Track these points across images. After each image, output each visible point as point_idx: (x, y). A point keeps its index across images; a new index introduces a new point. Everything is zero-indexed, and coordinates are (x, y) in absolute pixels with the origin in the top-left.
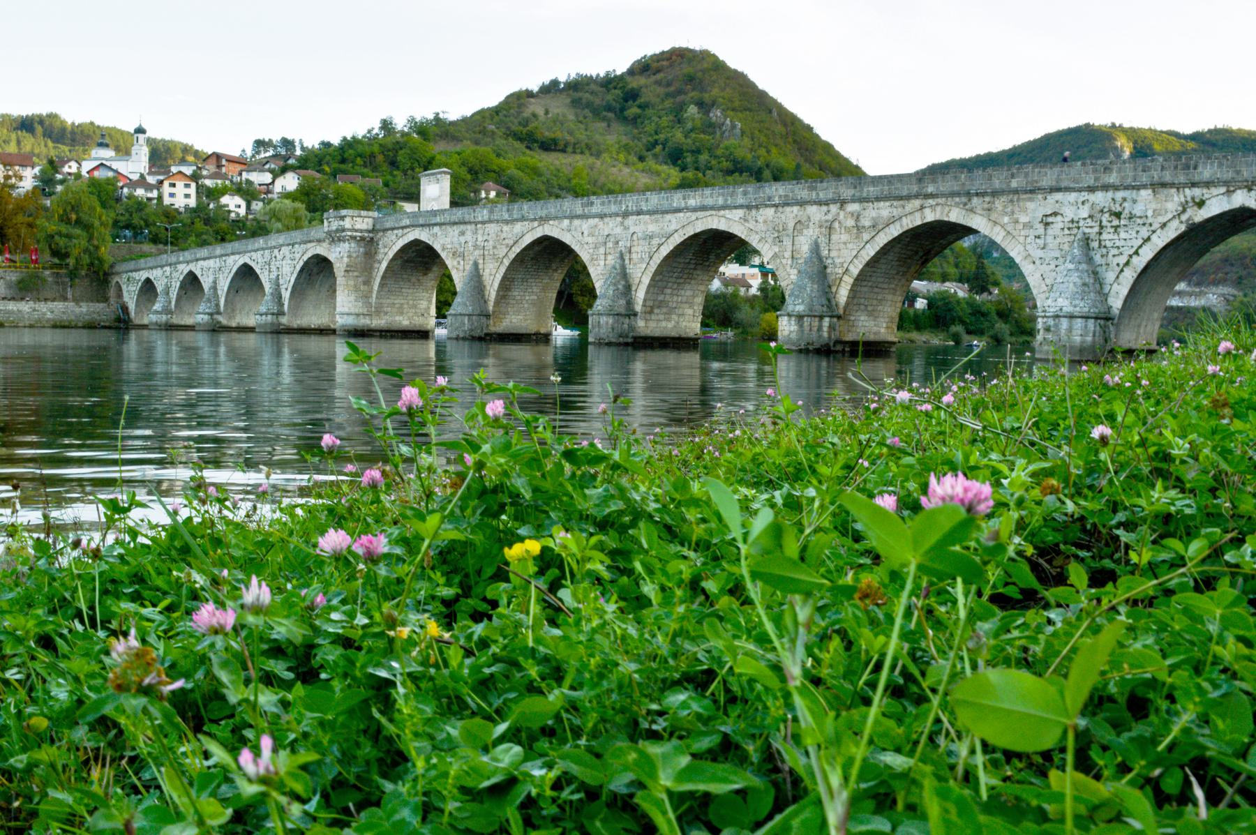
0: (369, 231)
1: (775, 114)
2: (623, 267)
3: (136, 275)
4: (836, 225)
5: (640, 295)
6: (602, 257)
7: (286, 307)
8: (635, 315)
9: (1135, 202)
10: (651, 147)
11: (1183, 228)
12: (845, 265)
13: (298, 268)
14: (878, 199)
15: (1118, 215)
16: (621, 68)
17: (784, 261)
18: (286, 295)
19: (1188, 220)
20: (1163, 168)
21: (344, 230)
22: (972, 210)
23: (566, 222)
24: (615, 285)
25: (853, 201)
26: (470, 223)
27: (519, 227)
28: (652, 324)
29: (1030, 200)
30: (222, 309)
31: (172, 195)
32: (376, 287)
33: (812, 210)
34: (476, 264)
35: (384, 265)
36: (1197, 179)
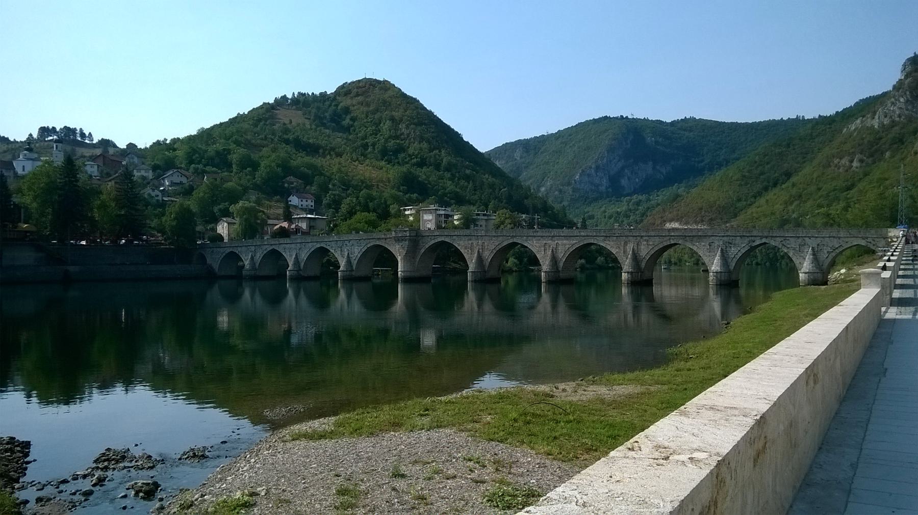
0: (415, 236)
3: (222, 250)
5: (561, 265)
7: (354, 267)
8: (559, 271)
9: (736, 240)
10: (365, 146)
11: (749, 248)
15: (730, 243)
16: (331, 90)
18: (355, 263)
20: (743, 231)
21: (407, 236)
22: (686, 241)
33: (631, 238)
34: (478, 252)
35: (423, 251)
36: (752, 235)
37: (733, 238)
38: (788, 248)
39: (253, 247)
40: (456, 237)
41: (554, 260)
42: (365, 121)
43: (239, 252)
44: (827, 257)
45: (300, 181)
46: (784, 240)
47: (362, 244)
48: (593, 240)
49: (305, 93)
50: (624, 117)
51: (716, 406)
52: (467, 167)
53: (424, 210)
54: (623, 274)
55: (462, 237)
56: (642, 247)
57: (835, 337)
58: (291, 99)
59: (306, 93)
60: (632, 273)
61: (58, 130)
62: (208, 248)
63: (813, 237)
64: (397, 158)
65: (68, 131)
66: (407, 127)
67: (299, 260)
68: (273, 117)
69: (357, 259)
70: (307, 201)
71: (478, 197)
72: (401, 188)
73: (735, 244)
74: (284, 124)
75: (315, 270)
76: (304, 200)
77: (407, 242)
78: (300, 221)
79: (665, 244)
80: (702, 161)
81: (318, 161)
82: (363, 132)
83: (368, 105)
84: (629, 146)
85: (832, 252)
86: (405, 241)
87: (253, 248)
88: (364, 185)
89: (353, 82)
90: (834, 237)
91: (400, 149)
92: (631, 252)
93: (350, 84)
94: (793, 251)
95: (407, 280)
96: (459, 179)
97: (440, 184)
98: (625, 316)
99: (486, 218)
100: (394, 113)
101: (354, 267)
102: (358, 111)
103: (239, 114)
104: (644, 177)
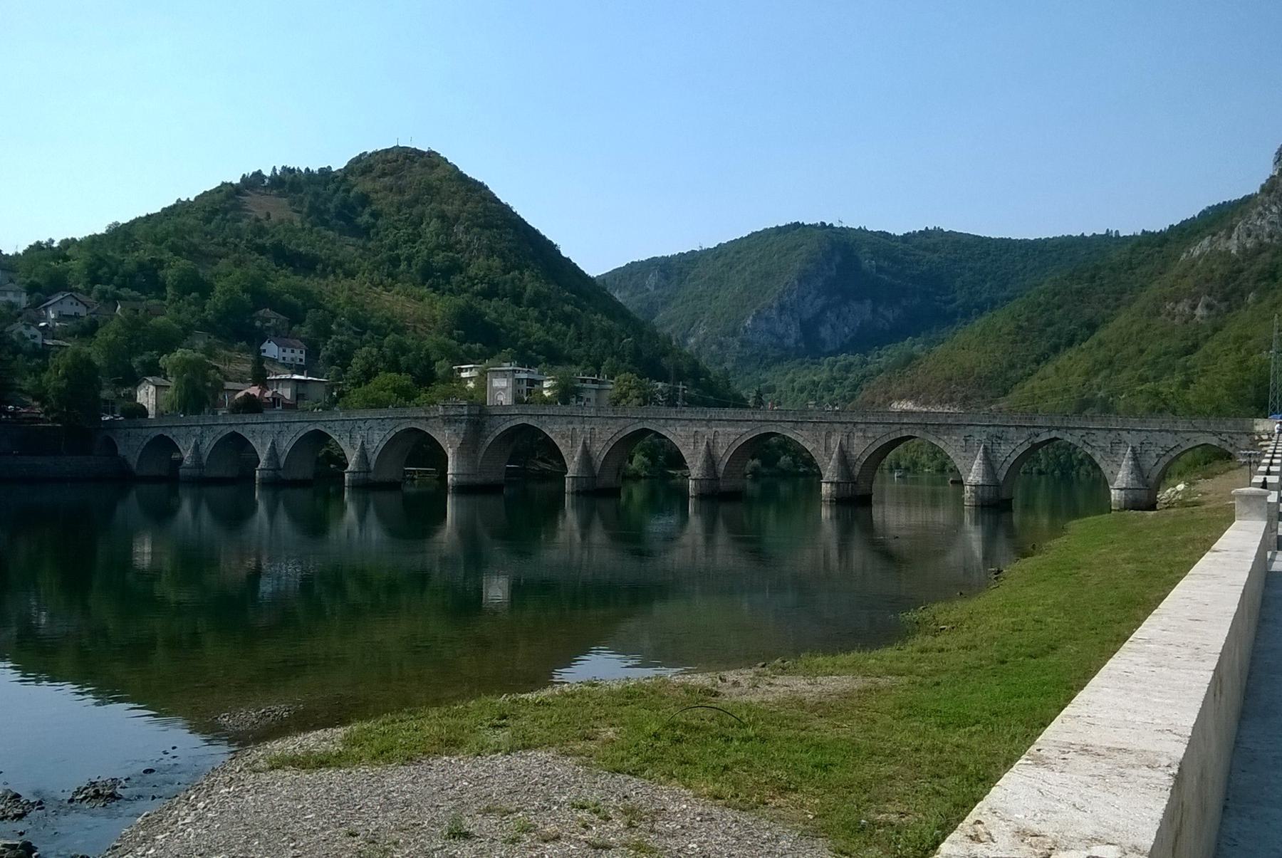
3: (144, 432)
4: (852, 434)
5: (722, 468)
7: (372, 466)
10: (395, 261)
13: (389, 437)
14: (876, 423)
16: (338, 164)
18: (373, 458)
21: (463, 415)
25: (861, 423)
27: (622, 421)
29: (958, 429)
32: (481, 455)
33: (838, 425)
34: (584, 443)
35: (490, 440)
37: (1004, 429)
38: (1093, 447)
39: (199, 428)
41: (711, 459)
42: (396, 218)
43: (174, 436)
44: (1156, 464)
45: (282, 317)
46: (1087, 434)
47: (387, 427)
49: (294, 169)
50: (827, 224)
51: (1091, 746)
52: (567, 301)
53: (493, 371)
54: (824, 485)
56: (856, 441)
57: (1234, 608)
58: (270, 178)
59: (296, 168)
60: (838, 484)
62: (120, 428)
63: (1133, 430)
64: (449, 283)
66: (467, 231)
67: (278, 452)
68: (238, 207)
69: (377, 453)
70: (293, 351)
71: (585, 351)
72: (455, 332)
73: (1007, 439)
74: (257, 220)
75: (304, 470)
76: (288, 350)
77: (464, 425)
78: (281, 384)
79: (893, 437)
80: (954, 300)
81: (312, 284)
82: (391, 237)
83: (401, 191)
84: (834, 273)
85: (1164, 455)
86: (461, 423)
87: (198, 430)
88: (392, 326)
89: (376, 153)
90: (1167, 431)
91: (455, 267)
92: (837, 450)
93: (370, 155)
94: (1102, 453)
95: (463, 490)
96: (552, 321)
97: (521, 329)
98: (826, 555)
99: (596, 386)
100: (445, 207)
101: (372, 466)
102: (384, 202)
103: (179, 200)
104: (858, 325)
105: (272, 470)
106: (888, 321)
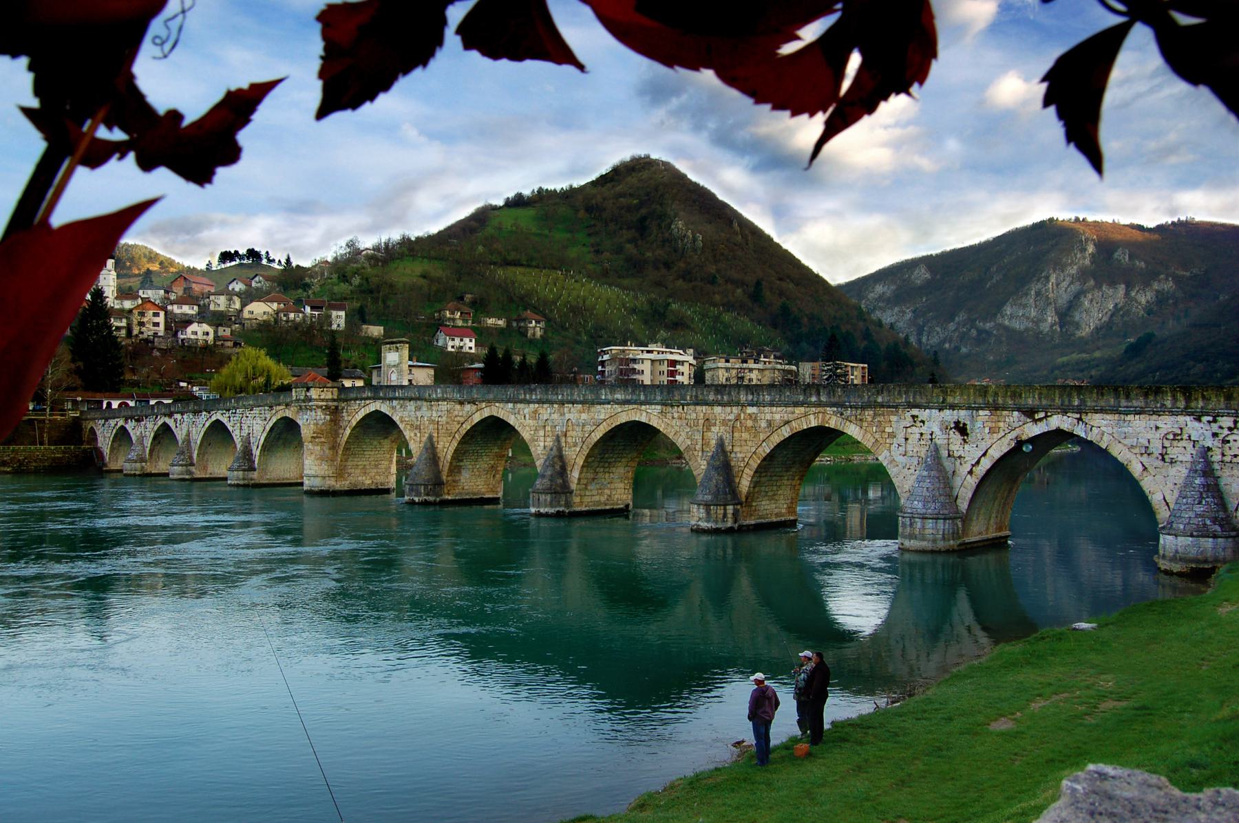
0: (334, 400)
1: (736, 225)
2: (560, 449)
6: (542, 439)
8: (571, 492)
12: (746, 460)
13: (268, 429)
17: (696, 453)
18: (256, 452)
19: (1016, 438)
23: (510, 405)
24: (553, 466)
26: (426, 400)
27: (468, 407)
28: (587, 500)
30: (195, 461)
31: (141, 324)
33: (718, 409)
34: (430, 438)
35: (348, 431)
40: (397, 402)
48: (638, 414)
50: (1081, 219)
55: (407, 403)
61: (241, 253)
65: (253, 254)
84: (1087, 262)
86: (311, 410)
94: (1145, 459)
99: (760, 366)
105: (182, 465)
106: (1140, 304)
